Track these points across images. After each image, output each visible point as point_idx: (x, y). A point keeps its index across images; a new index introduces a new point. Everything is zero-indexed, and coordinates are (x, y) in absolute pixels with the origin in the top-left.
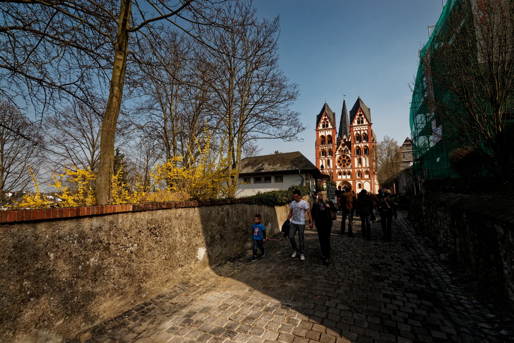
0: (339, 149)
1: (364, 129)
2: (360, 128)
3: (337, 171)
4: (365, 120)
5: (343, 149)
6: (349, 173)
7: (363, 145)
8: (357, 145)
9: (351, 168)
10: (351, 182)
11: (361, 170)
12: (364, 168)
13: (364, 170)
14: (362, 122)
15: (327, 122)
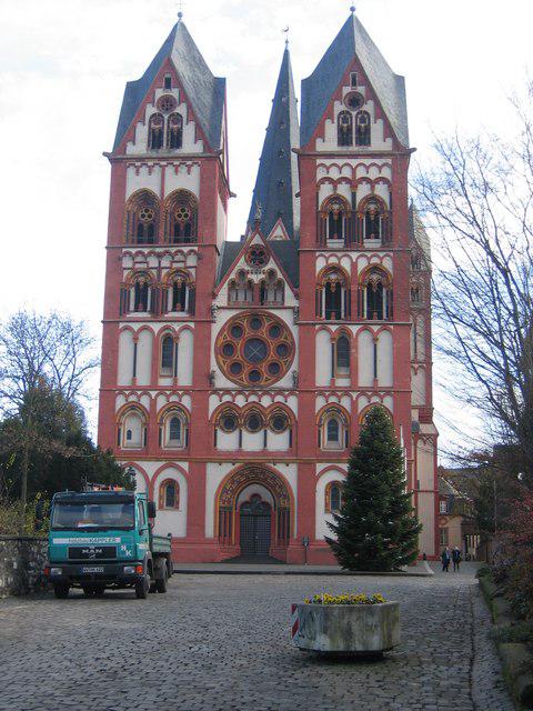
0: (232, 276)
1: (373, 174)
2: (354, 171)
3: (214, 402)
4: (377, 129)
5: (256, 278)
6: (280, 421)
7: (362, 264)
8: (333, 260)
9: (292, 392)
10: (289, 473)
11: (345, 403)
12: (363, 392)
13: (363, 403)
14: (364, 137)
15: (177, 118)
